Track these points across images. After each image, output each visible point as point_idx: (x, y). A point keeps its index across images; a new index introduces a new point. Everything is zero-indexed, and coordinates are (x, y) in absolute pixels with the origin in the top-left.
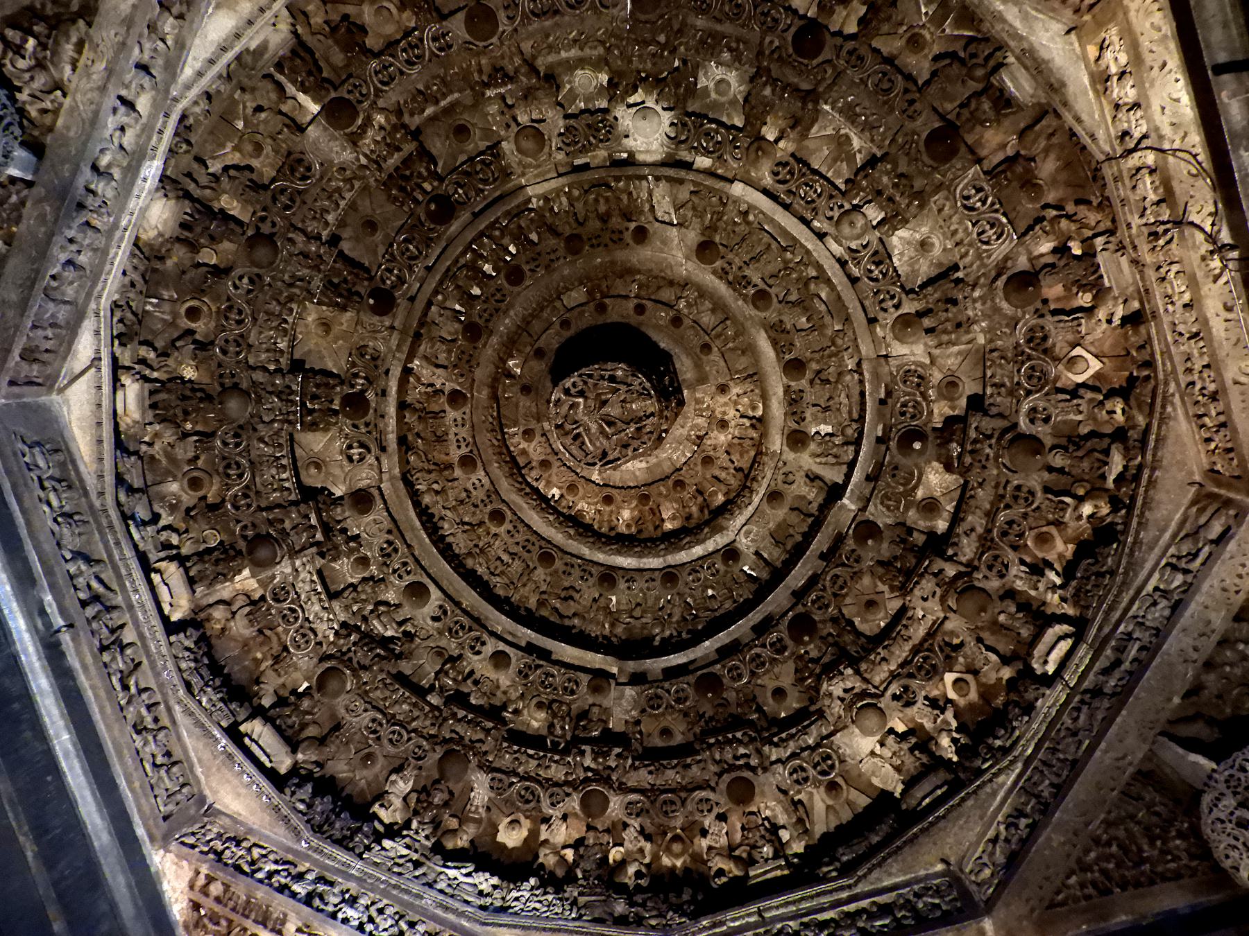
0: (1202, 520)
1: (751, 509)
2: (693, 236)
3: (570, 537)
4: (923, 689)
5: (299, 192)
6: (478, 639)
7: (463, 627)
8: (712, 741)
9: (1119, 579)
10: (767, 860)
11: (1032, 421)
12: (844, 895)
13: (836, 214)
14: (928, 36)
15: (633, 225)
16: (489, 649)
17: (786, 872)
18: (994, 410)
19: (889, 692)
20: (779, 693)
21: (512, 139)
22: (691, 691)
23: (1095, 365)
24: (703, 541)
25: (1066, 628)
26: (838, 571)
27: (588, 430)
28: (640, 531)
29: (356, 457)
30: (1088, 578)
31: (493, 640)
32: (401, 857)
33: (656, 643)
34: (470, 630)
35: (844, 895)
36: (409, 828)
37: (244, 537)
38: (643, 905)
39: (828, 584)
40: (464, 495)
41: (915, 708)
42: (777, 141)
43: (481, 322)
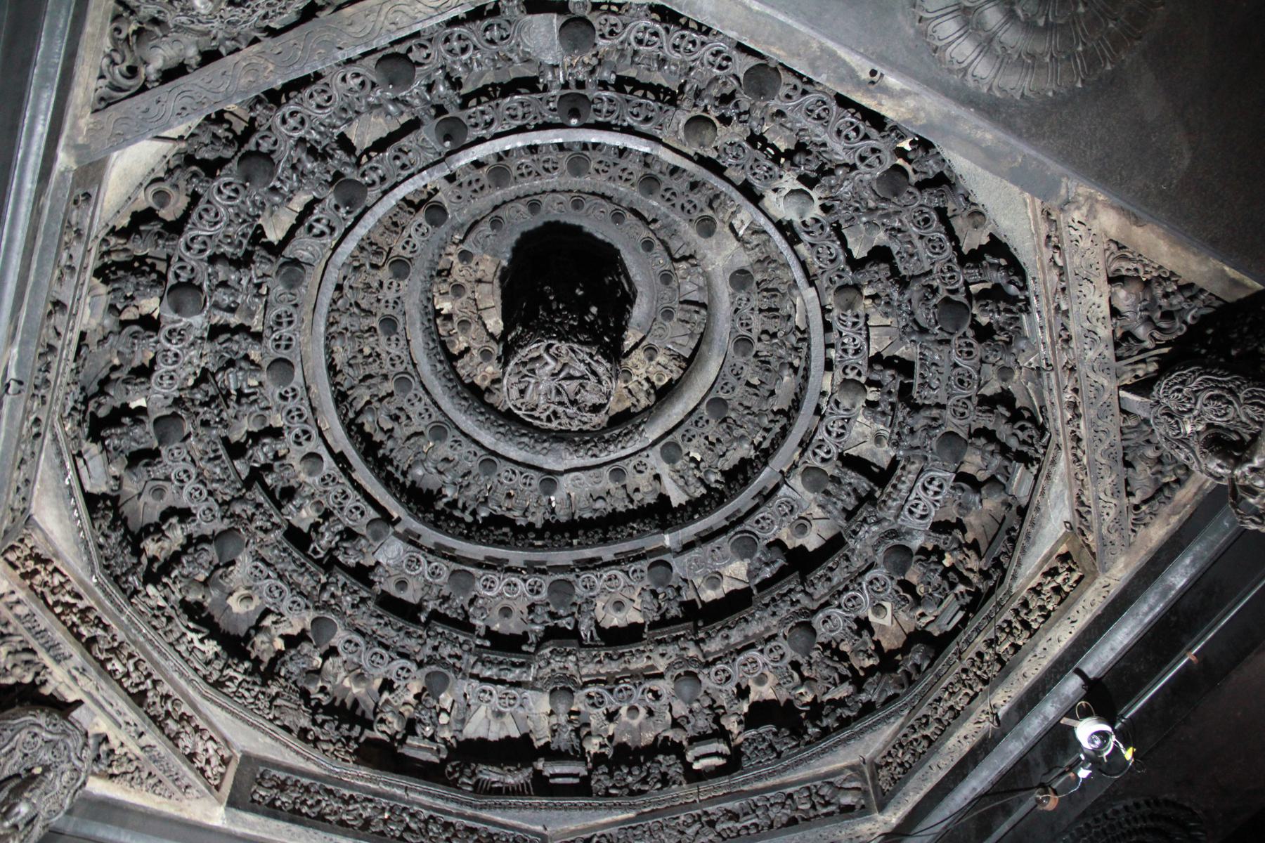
0: (847, 785)
1: (594, 461)
2: (744, 260)
3: (436, 373)
4: (611, 702)
5: (475, 48)
6: (305, 432)
7: (300, 416)
8: (440, 630)
9: (779, 766)
10: (424, 737)
11: (824, 622)
12: (469, 811)
13: (851, 375)
14: (1016, 377)
15: (709, 212)
16: (308, 447)
17: (435, 759)
18: (810, 590)
19: (587, 691)
20: (506, 612)
21: (689, 116)
22: (445, 574)
23: (887, 620)
24: (539, 453)
25: (723, 748)
26: (620, 575)
27: (537, 383)
28: (488, 390)
29: (315, 231)
30: (764, 740)
31: (320, 441)
32: (160, 608)
33: (440, 505)
34: (306, 422)
35: (469, 811)
36: (168, 575)
37: (177, 276)
38: (321, 726)
39: (605, 576)
40: (376, 285)
41: (595, 711)
42: (867, 297)
43: (515, 173)
